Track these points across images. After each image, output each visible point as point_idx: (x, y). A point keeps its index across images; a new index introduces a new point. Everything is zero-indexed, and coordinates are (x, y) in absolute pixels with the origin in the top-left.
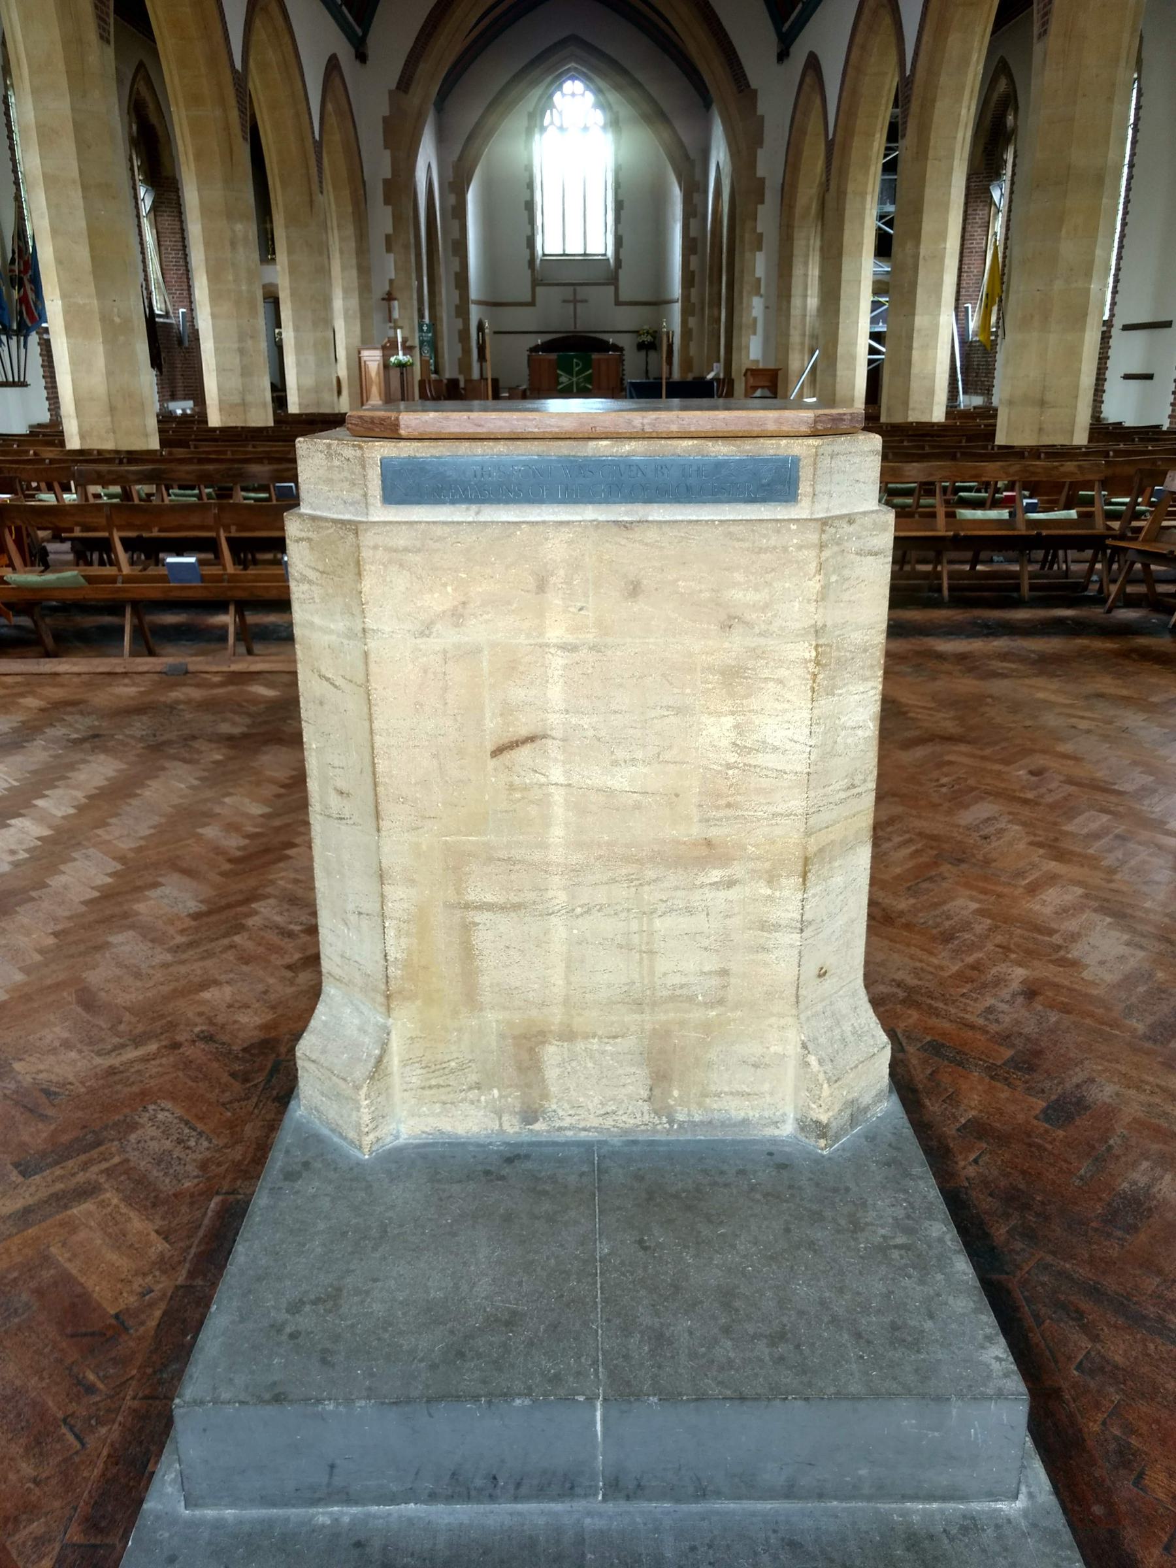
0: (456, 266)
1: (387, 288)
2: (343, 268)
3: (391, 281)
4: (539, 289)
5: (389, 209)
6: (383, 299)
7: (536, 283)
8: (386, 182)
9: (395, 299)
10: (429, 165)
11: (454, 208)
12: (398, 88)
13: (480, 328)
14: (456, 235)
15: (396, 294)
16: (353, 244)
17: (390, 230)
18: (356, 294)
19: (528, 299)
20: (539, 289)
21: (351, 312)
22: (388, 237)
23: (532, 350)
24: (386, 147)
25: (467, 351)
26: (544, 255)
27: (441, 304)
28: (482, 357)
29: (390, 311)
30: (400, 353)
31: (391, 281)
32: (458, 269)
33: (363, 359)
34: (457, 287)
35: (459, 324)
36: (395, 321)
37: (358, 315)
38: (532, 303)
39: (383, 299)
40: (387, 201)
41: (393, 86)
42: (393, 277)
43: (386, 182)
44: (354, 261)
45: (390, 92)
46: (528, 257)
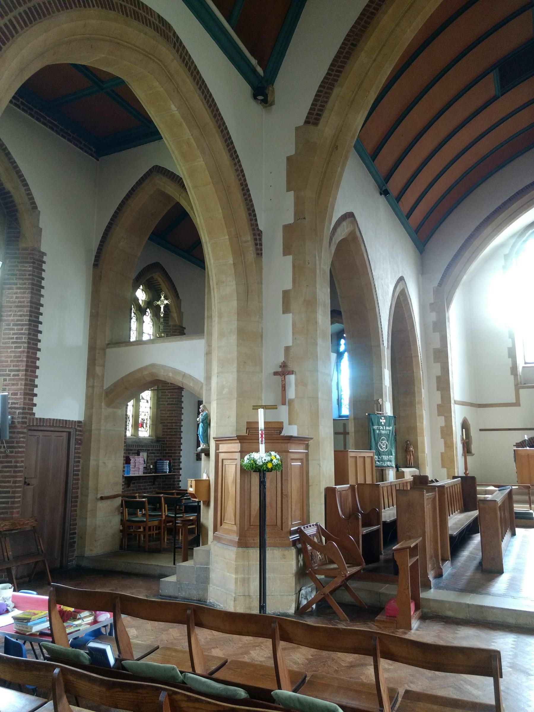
0: (437, 370)
1: (282, 359)
2: (222, 334)
3: (287, 349)
4: (521, 391)
5: (290, 258)
6: (276, 374)
7: (519, 386)
8: (287, 228)
9: (292, 373)
10: (401, 279)
11: (435, 324)
12: (307, 122)
13: (465, 426)
14: (438, 346)
15: (291, 366)
16: (235, 304)
17: (289, 286)
18: (234, 368)
19: (514, 401)
20: (521, 391)
21: (226, 391)
22: (286, 294)
23: (518, 445)
24: (288, 190)
25: (449, 445)
26: (526, 363)
27: (420, 403)
28: (467, 450)
29: (284, 388)
30: (262, 447)
31: (287, 349)
32: (439, 374)
33: (222, 456)
34: (438, 389)
35: (441, 421)
36: (291, 402)
37: (235, 395)
38: (517, 404)
39: (276, 374)
40: (286, 251)
41: (301, 122)
42: (290, 344)
43: (287, 228)
44: (234, 325)
45: (297, 129)
46: (510, 365)
